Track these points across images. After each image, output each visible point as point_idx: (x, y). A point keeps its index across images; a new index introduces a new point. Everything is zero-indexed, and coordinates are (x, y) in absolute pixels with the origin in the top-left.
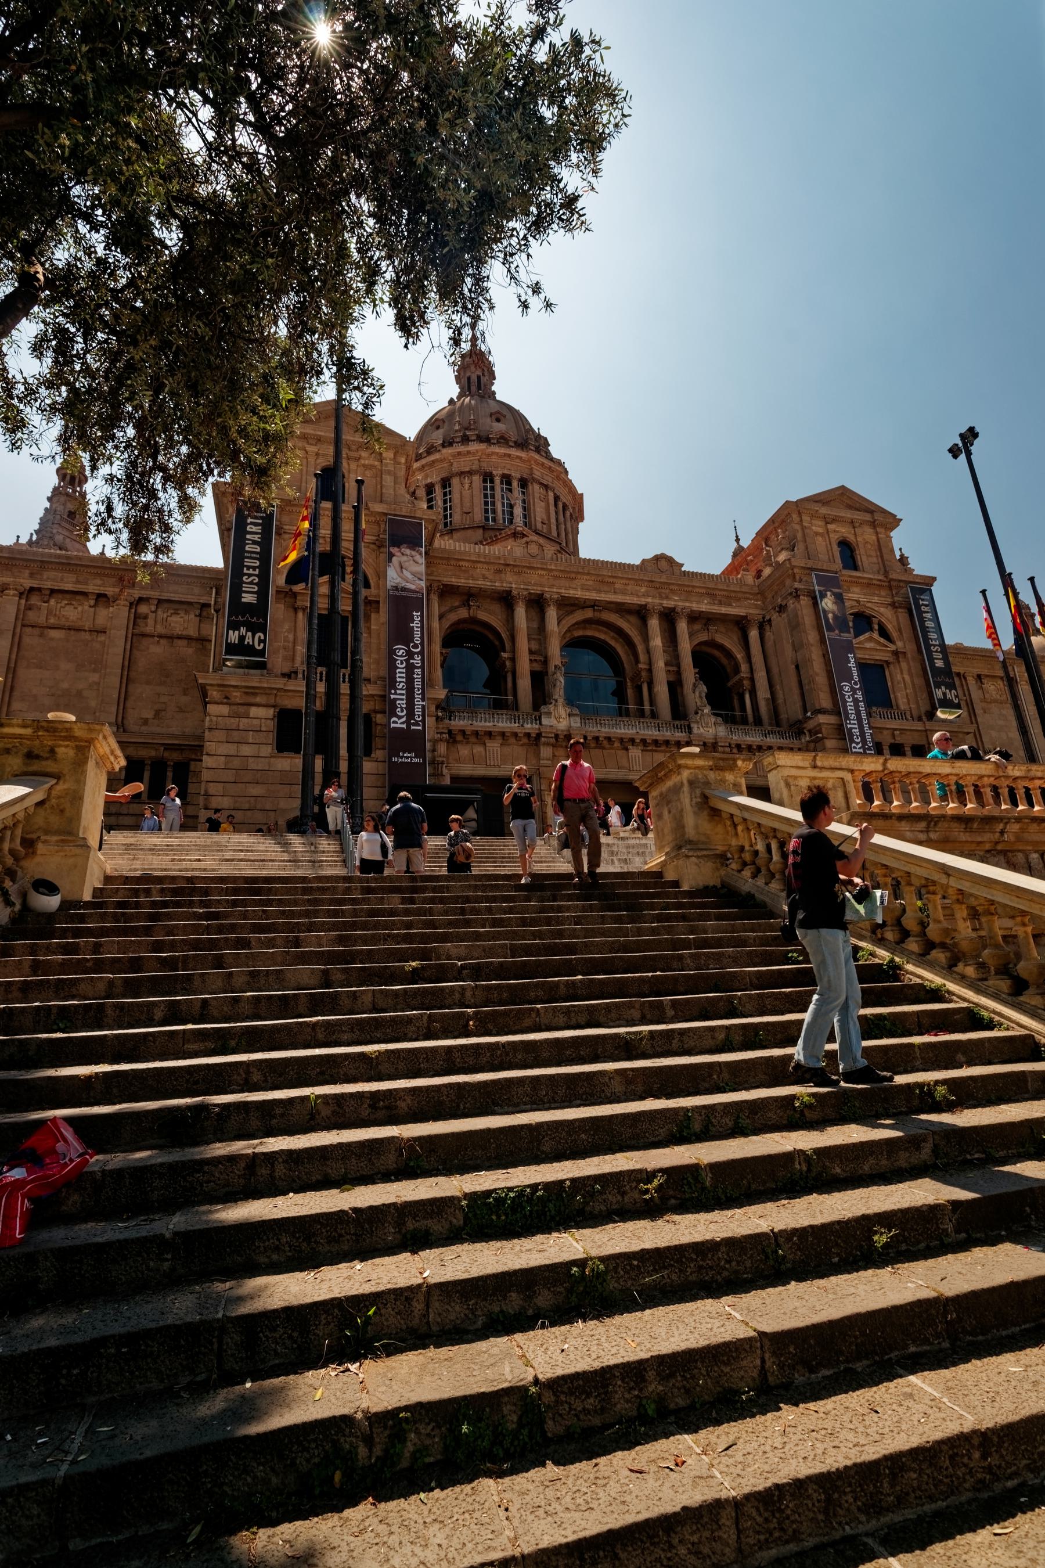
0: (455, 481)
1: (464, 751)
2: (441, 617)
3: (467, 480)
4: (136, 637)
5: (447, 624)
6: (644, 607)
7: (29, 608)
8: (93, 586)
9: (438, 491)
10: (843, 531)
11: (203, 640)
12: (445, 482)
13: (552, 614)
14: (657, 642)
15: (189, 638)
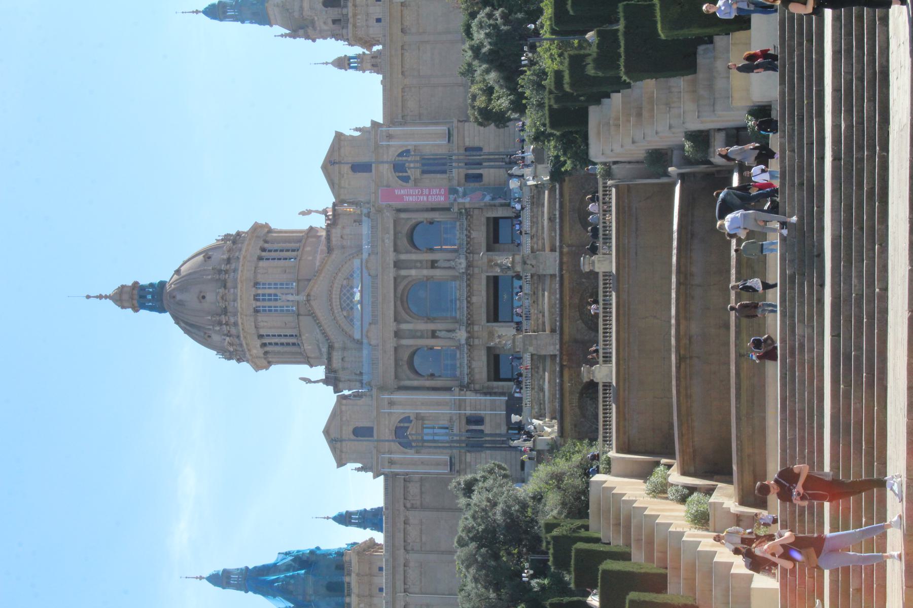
0: (262, 332)
1: (477, 377)
2: (409, 379)
3: (262, 324)
4: (423, 508)
5: (412, 376)
6: (395, 279)
7: (413, 550)
8: (401, 526)
9: (267, 341)
10: (346, 169)
11: (421, 480)
12: (261, 336)
13: (404, 326)
14: (413, 272)
15: (421, 486)
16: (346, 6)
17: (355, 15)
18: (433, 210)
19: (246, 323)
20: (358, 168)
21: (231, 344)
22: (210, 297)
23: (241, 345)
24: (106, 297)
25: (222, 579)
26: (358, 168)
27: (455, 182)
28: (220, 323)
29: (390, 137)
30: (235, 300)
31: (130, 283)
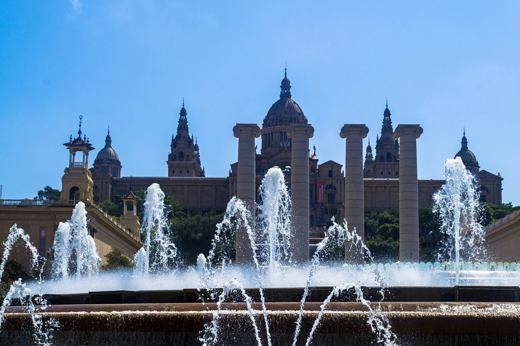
0: (274, 134)
9: (270, 135)
10: (331, 169)
12: (272, 133)
16: (387, 161)
17: (384, 164)
18: (316, 197)
19: (277, 128)
20: (330, 172)
21: (269, 122)
22: (286, 116)
23: (269, 126)
24: (286, 76)
25: (183, 112)
26: (330, 172)
27: (325, 205)
28: (277, 119)
29: (341, 183)
30: (285, 125)
31: (290, 85)
